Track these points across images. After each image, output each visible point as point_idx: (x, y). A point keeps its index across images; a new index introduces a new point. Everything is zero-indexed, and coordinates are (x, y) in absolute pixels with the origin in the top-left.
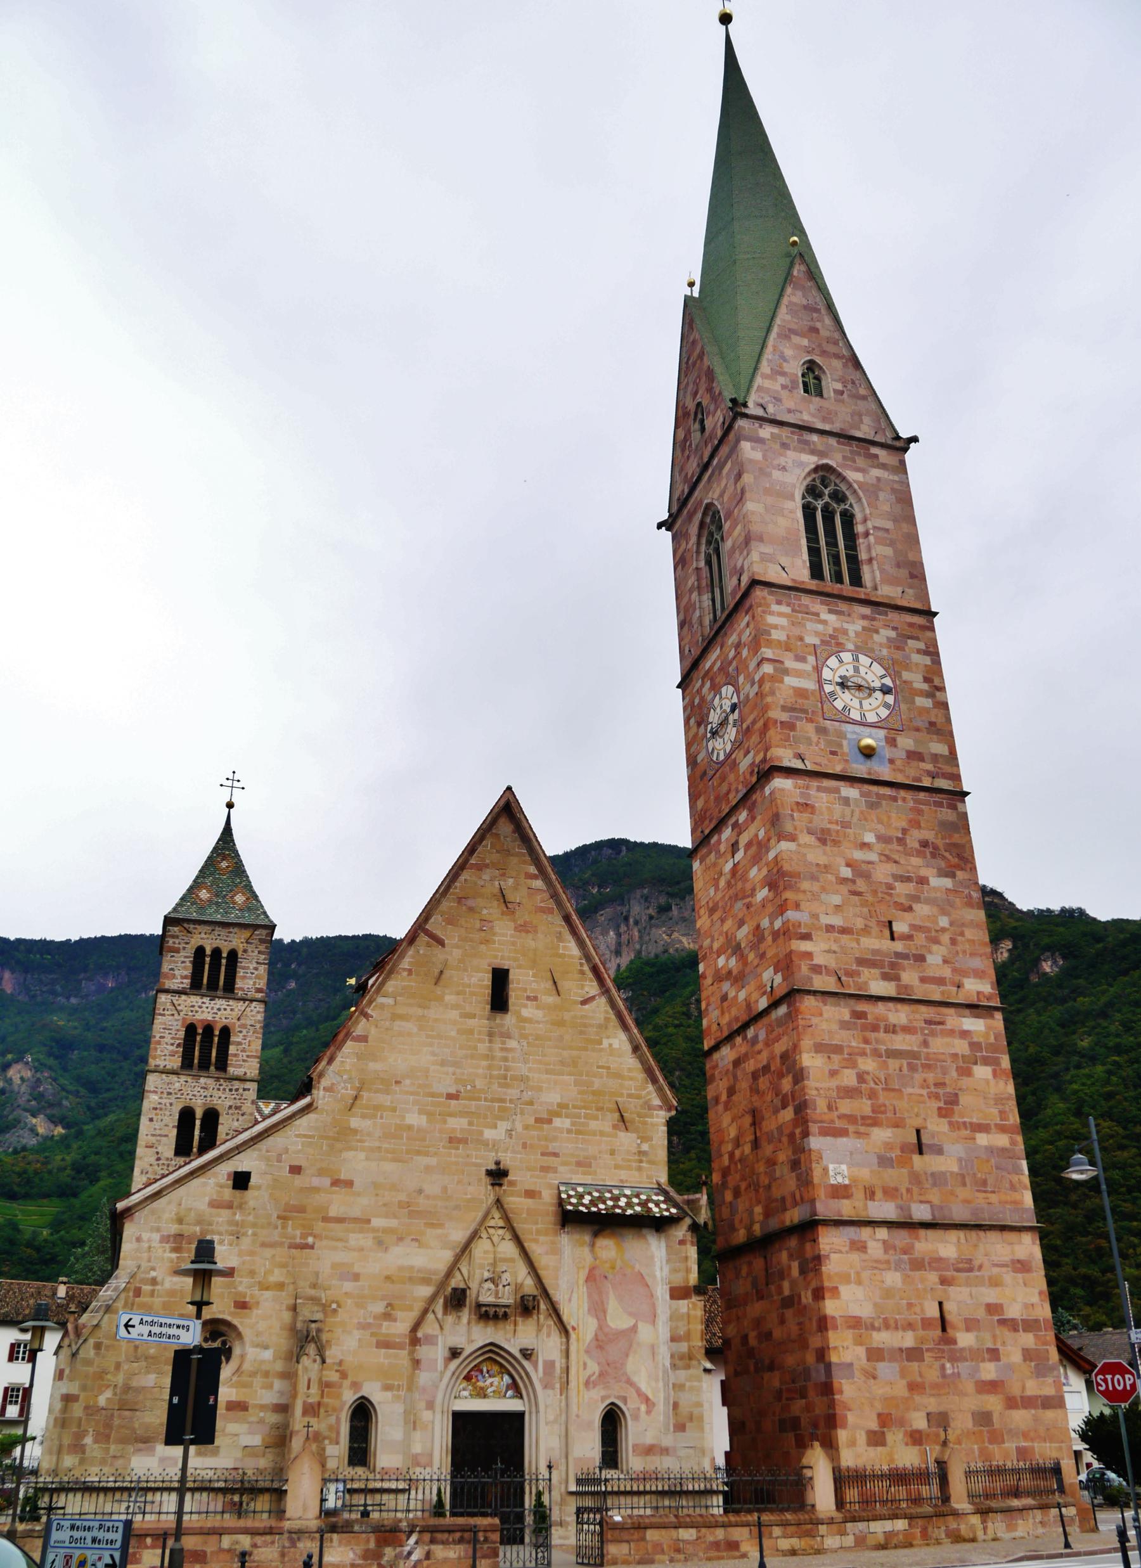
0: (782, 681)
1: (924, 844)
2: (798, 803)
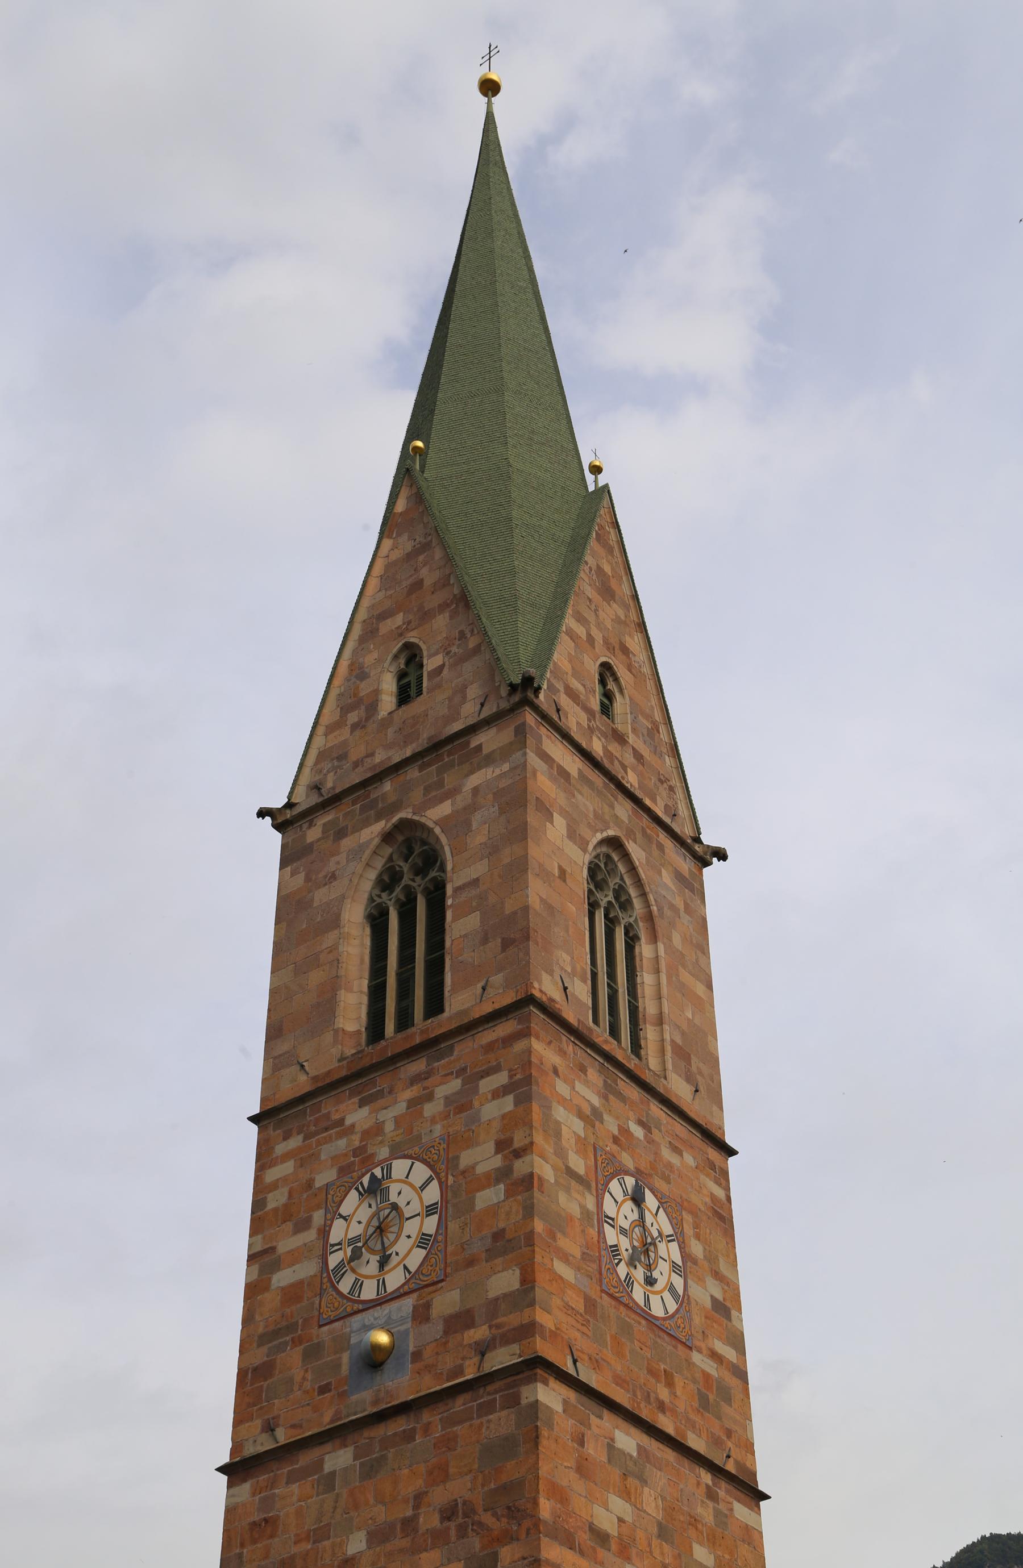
0: (267, 1288)
1: (448, 1513)
2: (254, 1524)
